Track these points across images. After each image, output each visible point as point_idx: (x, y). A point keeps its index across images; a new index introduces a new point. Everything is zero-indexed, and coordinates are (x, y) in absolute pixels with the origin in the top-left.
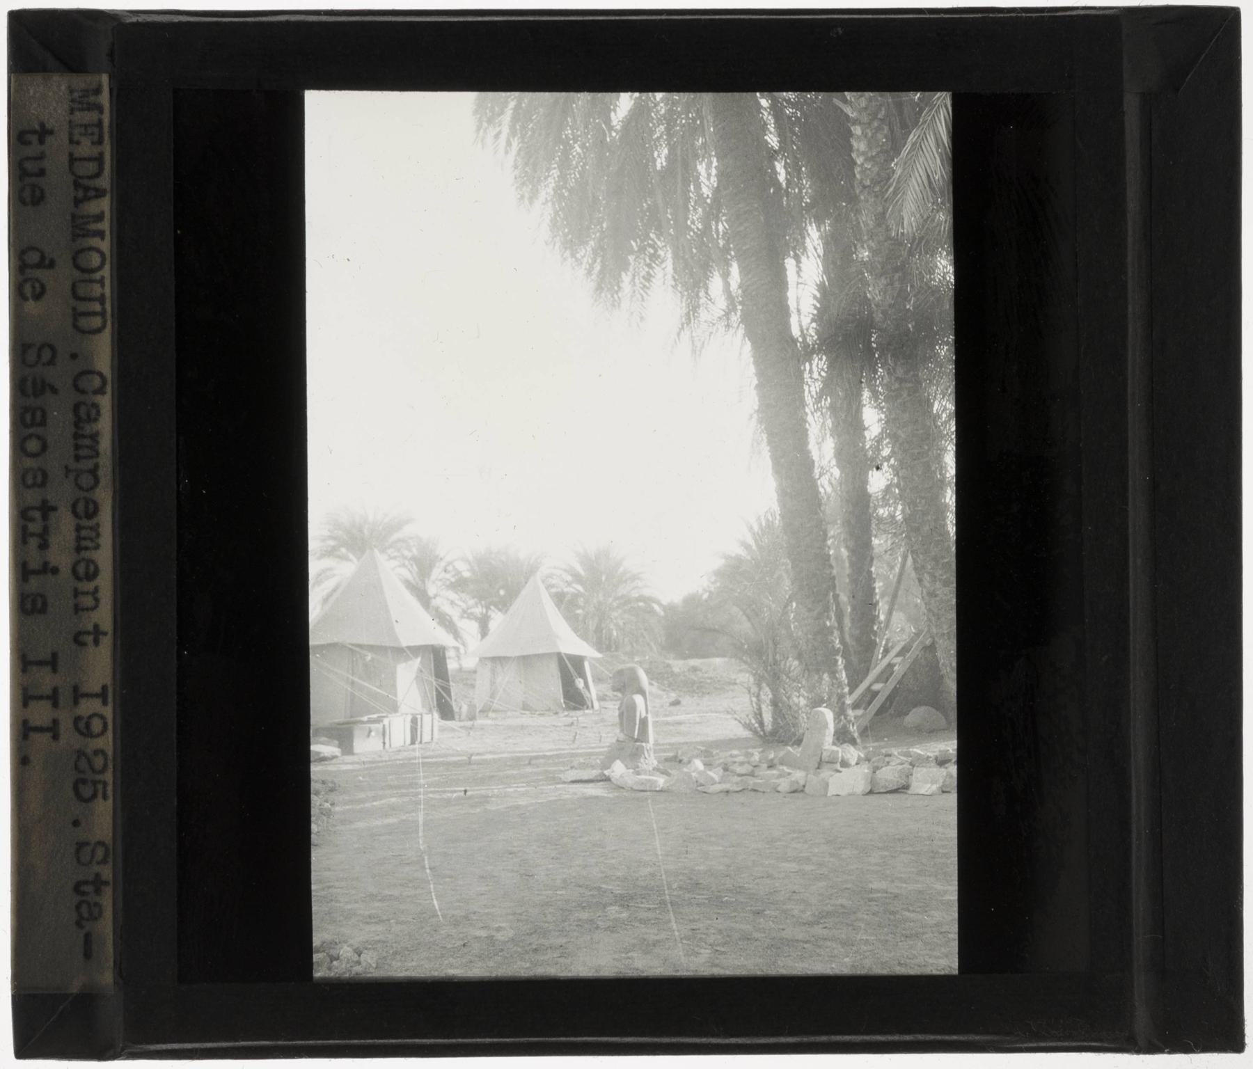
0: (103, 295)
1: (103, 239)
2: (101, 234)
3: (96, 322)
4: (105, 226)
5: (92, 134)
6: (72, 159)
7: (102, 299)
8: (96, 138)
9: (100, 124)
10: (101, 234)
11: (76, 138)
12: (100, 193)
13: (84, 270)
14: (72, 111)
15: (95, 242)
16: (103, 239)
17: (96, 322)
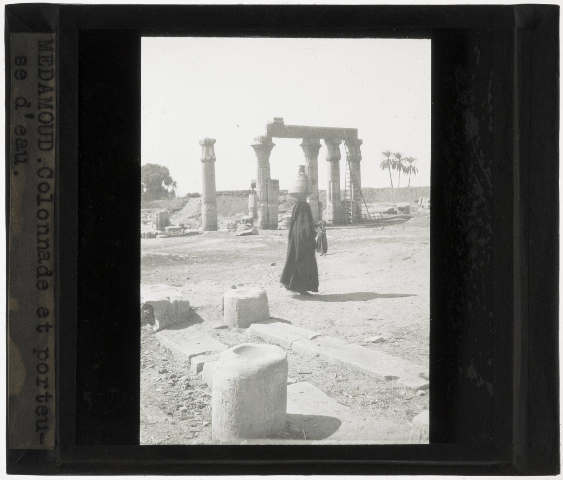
0: (52, 132)
1: (52, 109)
2: (51, 107)
3: (48, 146)
4: (53, 103)
5: (48, 61)
6: (40, 71)
7: (51, 134)
8: (50, 63)
9: (52, 57)
10: (51, 107)
11: (42, 62)
12: (52, 89)
13: (43, 122)
14: (39, 50)
15: (48, 110)
16: (52, 109)
17: (48, 146)
